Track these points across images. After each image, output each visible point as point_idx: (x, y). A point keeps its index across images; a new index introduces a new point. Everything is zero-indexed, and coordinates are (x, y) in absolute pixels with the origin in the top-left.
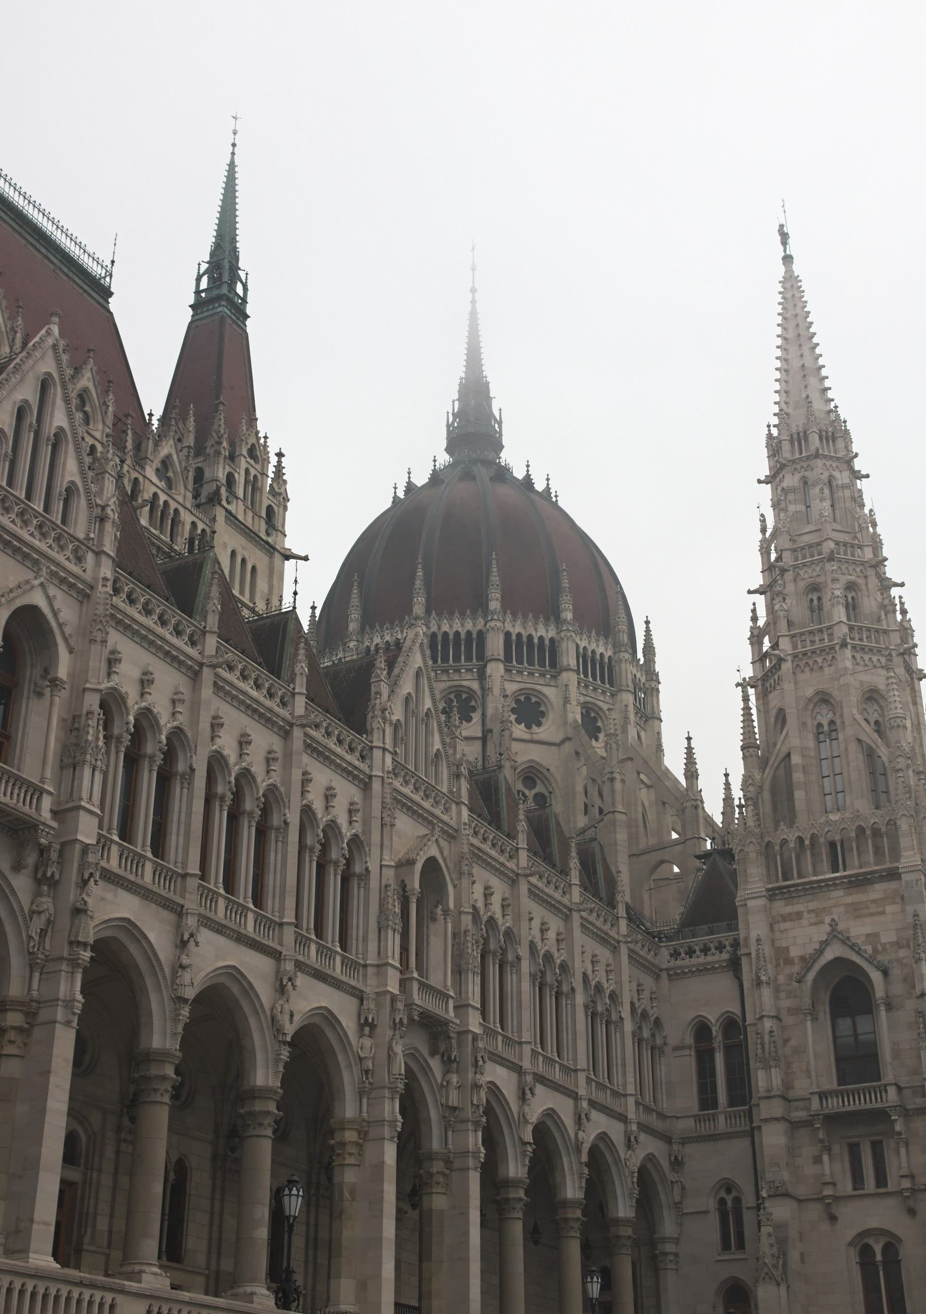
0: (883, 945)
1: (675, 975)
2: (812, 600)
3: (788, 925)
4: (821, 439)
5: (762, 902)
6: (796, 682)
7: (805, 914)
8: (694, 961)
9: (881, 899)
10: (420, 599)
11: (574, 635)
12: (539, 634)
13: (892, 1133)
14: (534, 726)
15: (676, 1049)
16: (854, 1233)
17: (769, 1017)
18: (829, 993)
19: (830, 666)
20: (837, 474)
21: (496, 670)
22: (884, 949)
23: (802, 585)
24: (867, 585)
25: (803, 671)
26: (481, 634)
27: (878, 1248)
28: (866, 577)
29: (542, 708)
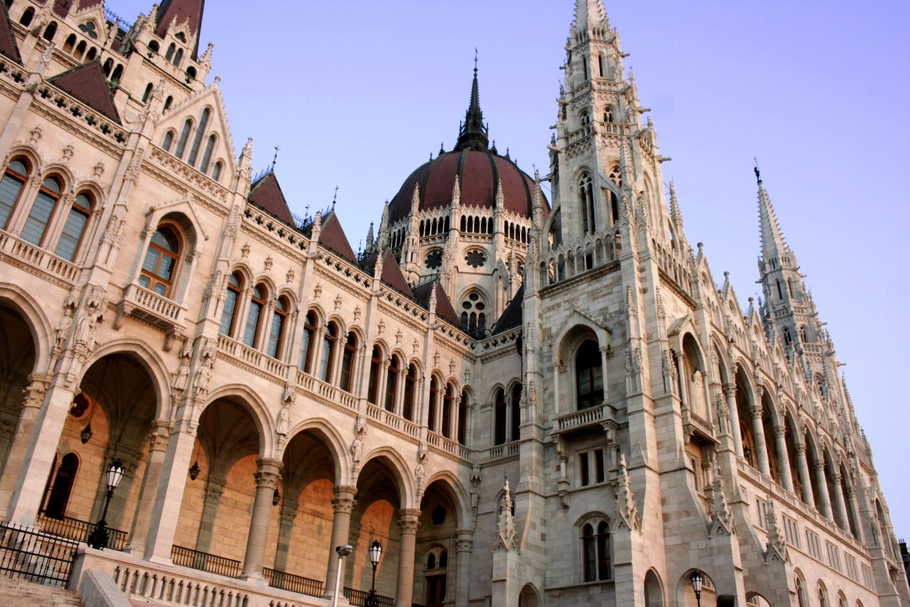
0: (610, 314)
1: (485, 359)
3: (552, 313)
4: (594, 33)
5: (536, 299)
6: (567, 165)
7: (563, 304)
8: (497, 348)
9: (611, 284)
13: (607, 442)
15: (483, 407)
16: (579, 516)
18: (574, 355)
20: (604, 50)
21: (455, 235)
22: (611, 317)
23: (576, 111)
24: (619, 105)
26: (448, 218)
27: (595, 527)
29: (484, 256)
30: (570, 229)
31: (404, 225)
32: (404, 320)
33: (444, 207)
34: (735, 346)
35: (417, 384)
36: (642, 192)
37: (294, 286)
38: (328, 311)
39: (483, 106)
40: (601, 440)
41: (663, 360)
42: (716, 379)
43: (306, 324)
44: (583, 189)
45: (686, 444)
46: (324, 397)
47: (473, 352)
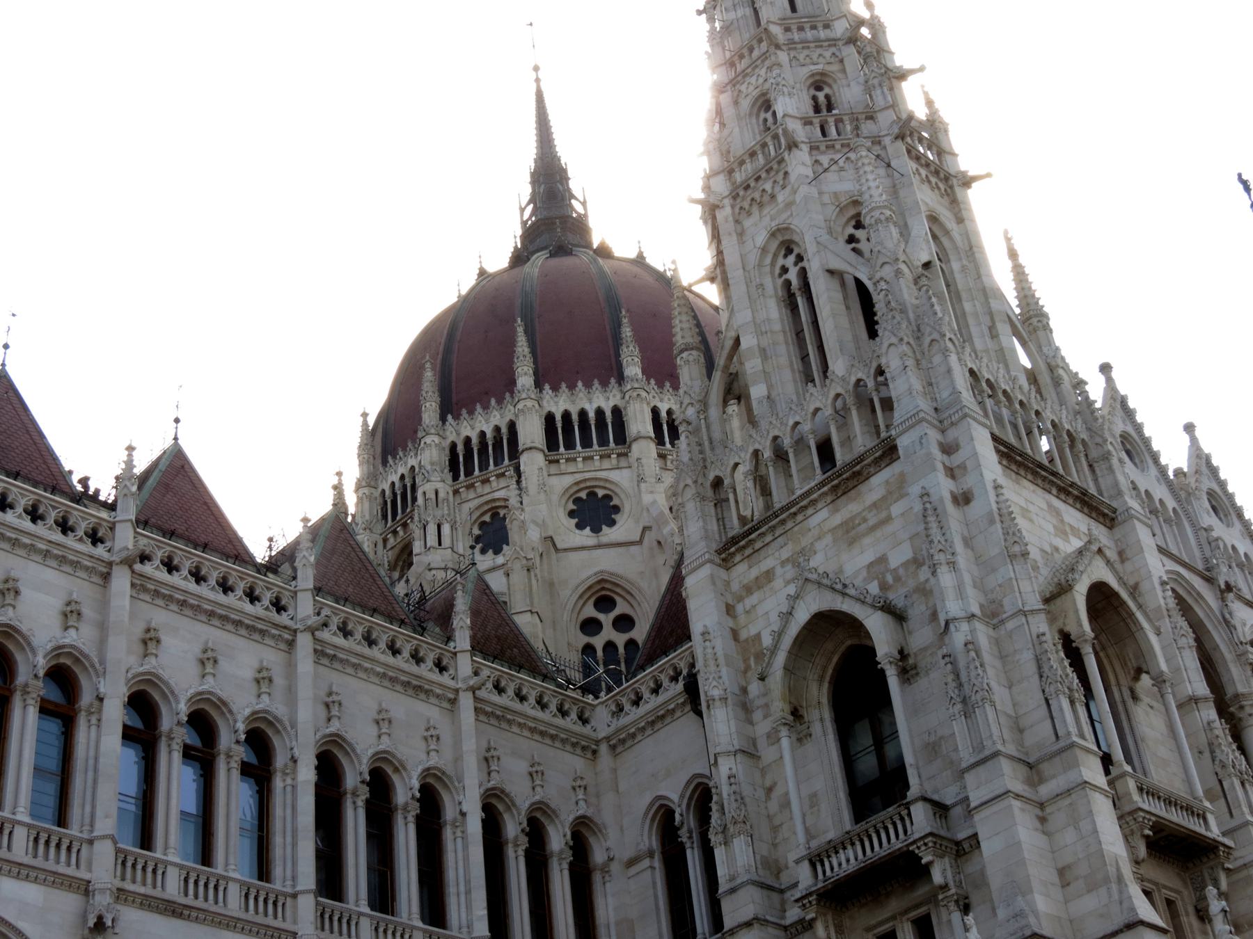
1: (619, 743)
2: (765, 120)
7: (779, 571)
8: (644, 709)
9: (884, 499)
10: (428, 405)
11: (644, 394)
12: (595, 406)
14: (604, 527)
15: (631, 863)
17: (728, 753)
19: (784, 187)
21: (532, 463)
22: (897, 579)
24: (844, 71)
25: (749, 214)
26: (512, 426)
28: (842, 61)
29: (615, 502)
30: (770, 387)
31: (412, 462)
32: (391, 680)
33: (500, 401)
34: (1240, 598)
35: (448, 833)
36: (927, 265)
37: (81, 638)
38: (182, 683)
39: (566, 153)
40: (922, 891)
41: (1038, 660)
42: (1200, 687)
43: (126, 728)
44: (788, 283)
45: (1137, 863)
46: (200, 903)
47: (586, 730)
